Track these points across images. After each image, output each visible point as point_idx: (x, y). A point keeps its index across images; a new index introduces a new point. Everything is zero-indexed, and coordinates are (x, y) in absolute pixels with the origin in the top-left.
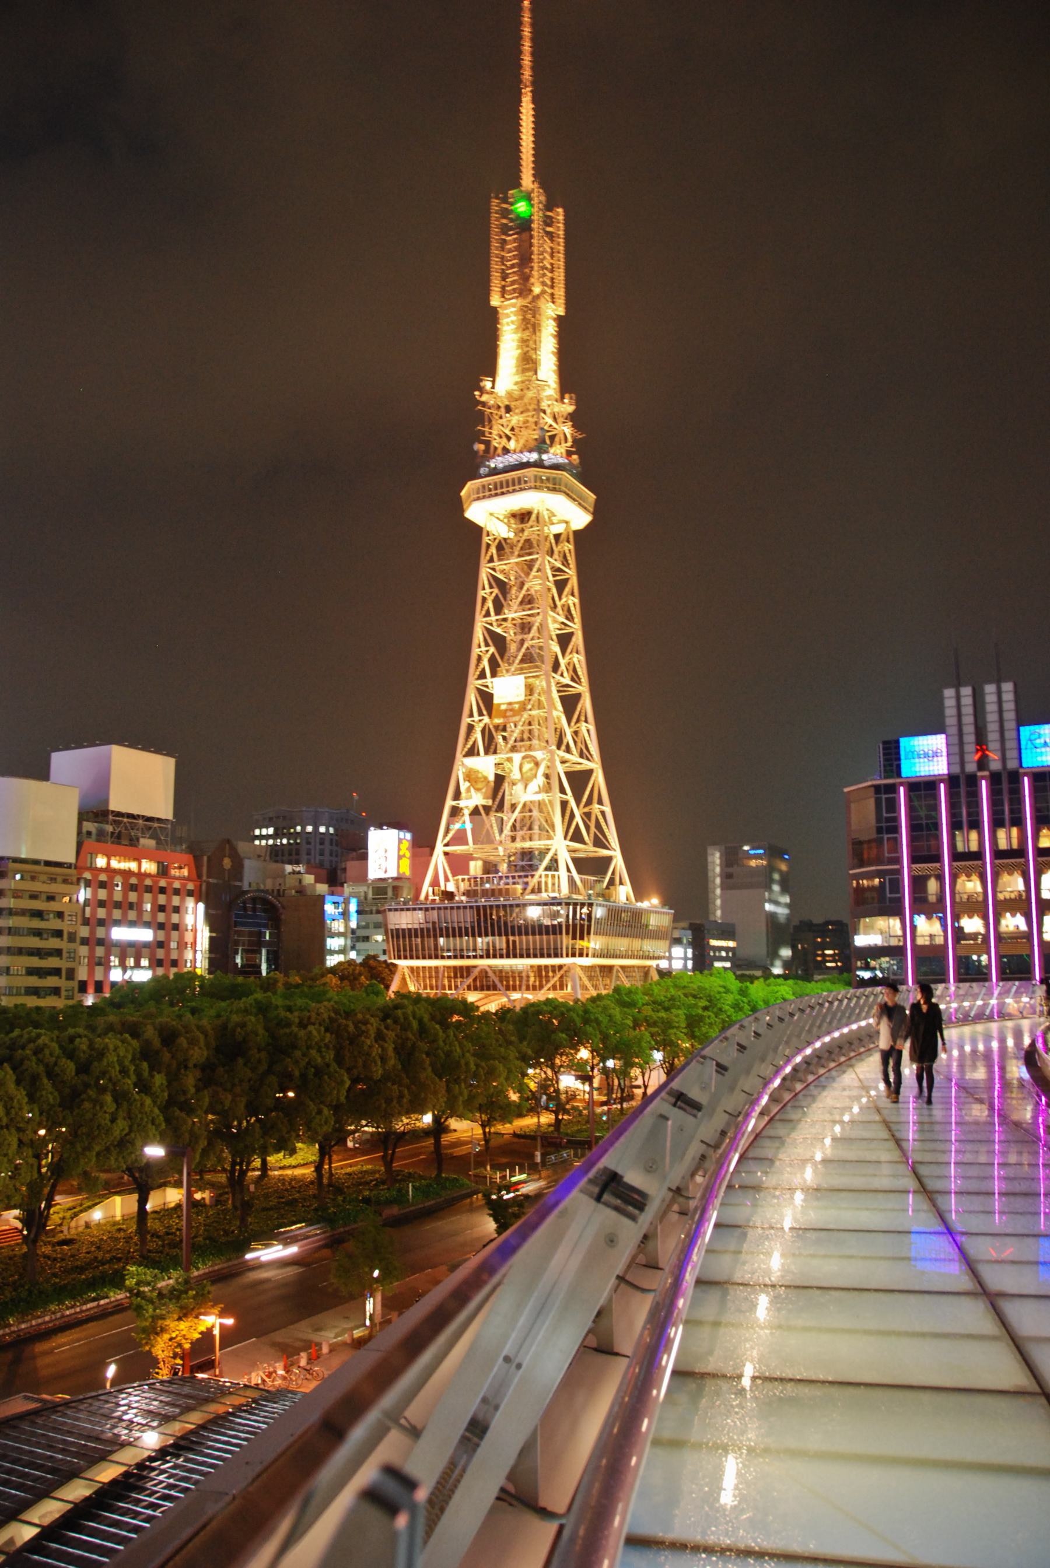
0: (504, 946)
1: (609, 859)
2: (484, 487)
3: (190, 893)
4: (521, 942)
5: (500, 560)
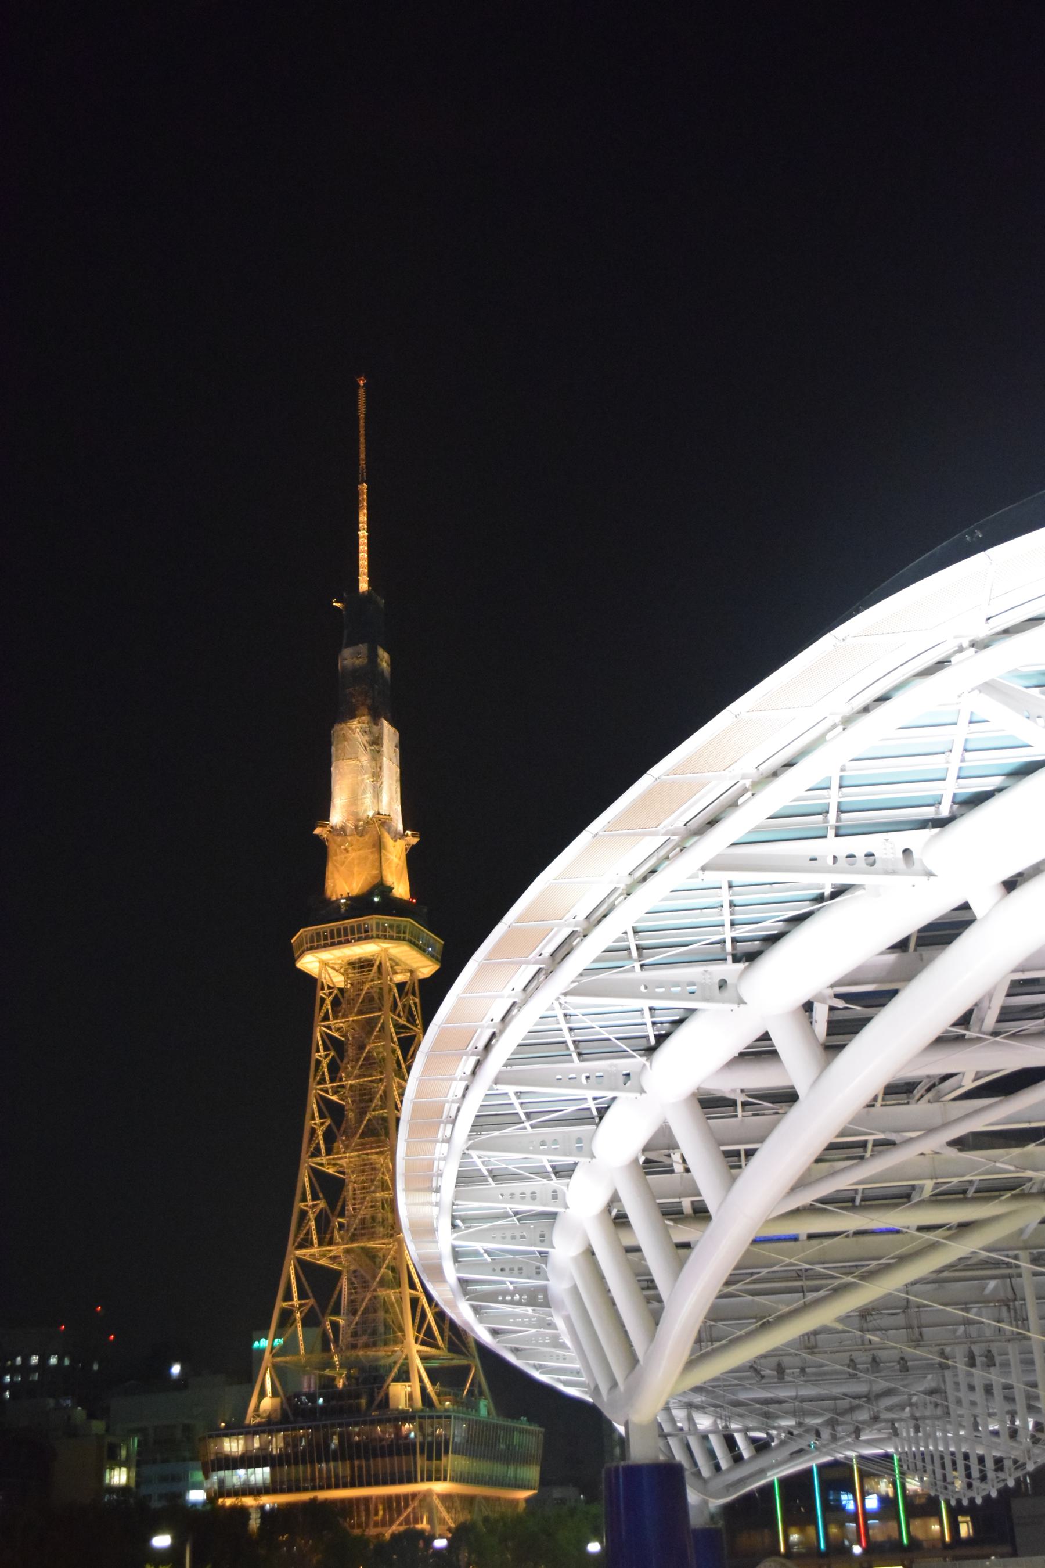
0: (348, 1472)
1: (467, 1369)
2: (318, 934)
4: (368, 1467)
5: (334, 1019)
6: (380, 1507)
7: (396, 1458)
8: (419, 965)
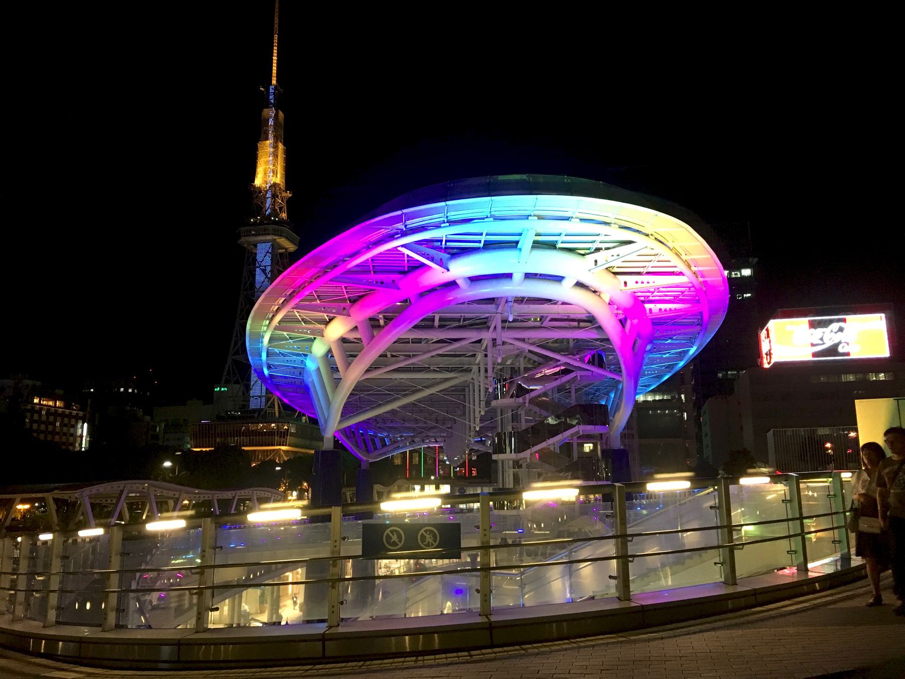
2: (247, 230)
3: (80, 418)
6: (260, 454)
7: (267, 437)
8: (289, 247)
